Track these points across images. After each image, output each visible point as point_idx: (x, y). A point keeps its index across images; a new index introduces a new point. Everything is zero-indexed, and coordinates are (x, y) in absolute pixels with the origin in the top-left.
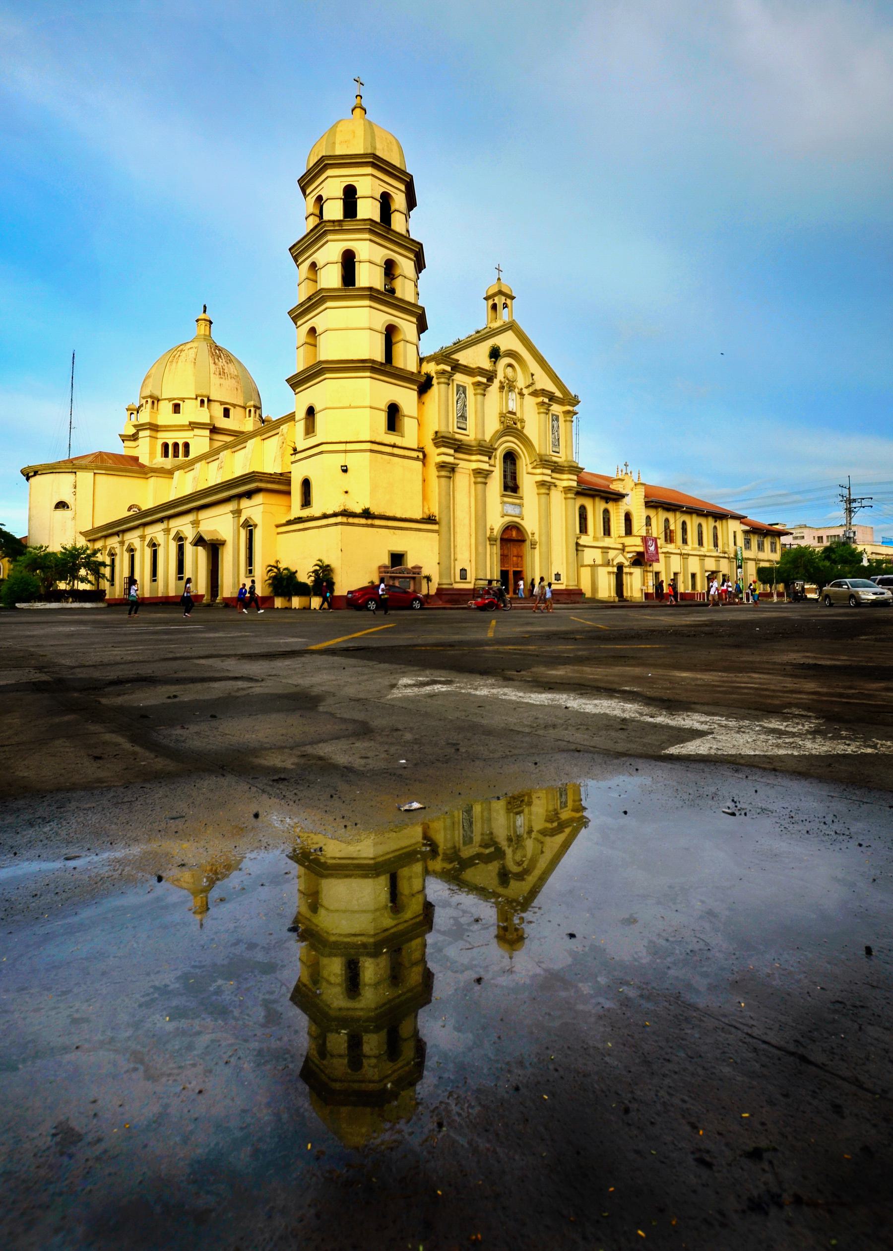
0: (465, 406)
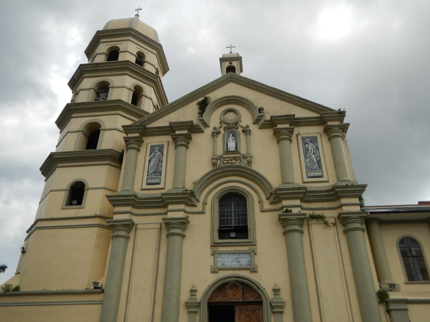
0: (160, 161)
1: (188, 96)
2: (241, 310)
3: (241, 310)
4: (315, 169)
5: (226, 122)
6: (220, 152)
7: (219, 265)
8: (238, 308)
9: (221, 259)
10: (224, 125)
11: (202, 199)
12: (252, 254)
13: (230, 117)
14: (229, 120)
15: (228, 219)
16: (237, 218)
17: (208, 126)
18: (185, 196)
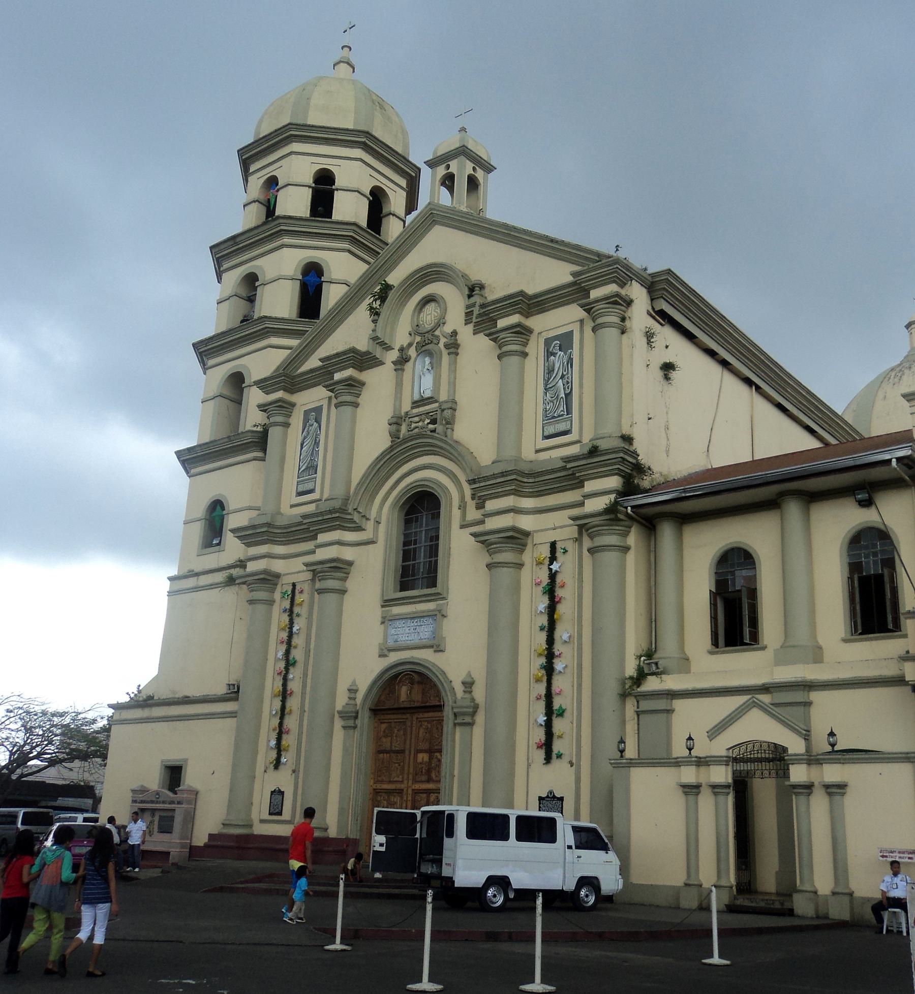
0: (317, 444)
1: (360, 281)
2: (420, 721)
3: (420, 721)
4: (559, 416)
5: (421, 330)
6: (406, 406)
7: (391, 643)
8: (417, 718)
9: (393, 631)
10: (418, 339)
11: (373, 514)
12: (439, 616)
13: (430, 314)
14: (426, 323)
15: (416, 548)
16: (429, 544)
17: (389, 348)
18: (334, 515)
